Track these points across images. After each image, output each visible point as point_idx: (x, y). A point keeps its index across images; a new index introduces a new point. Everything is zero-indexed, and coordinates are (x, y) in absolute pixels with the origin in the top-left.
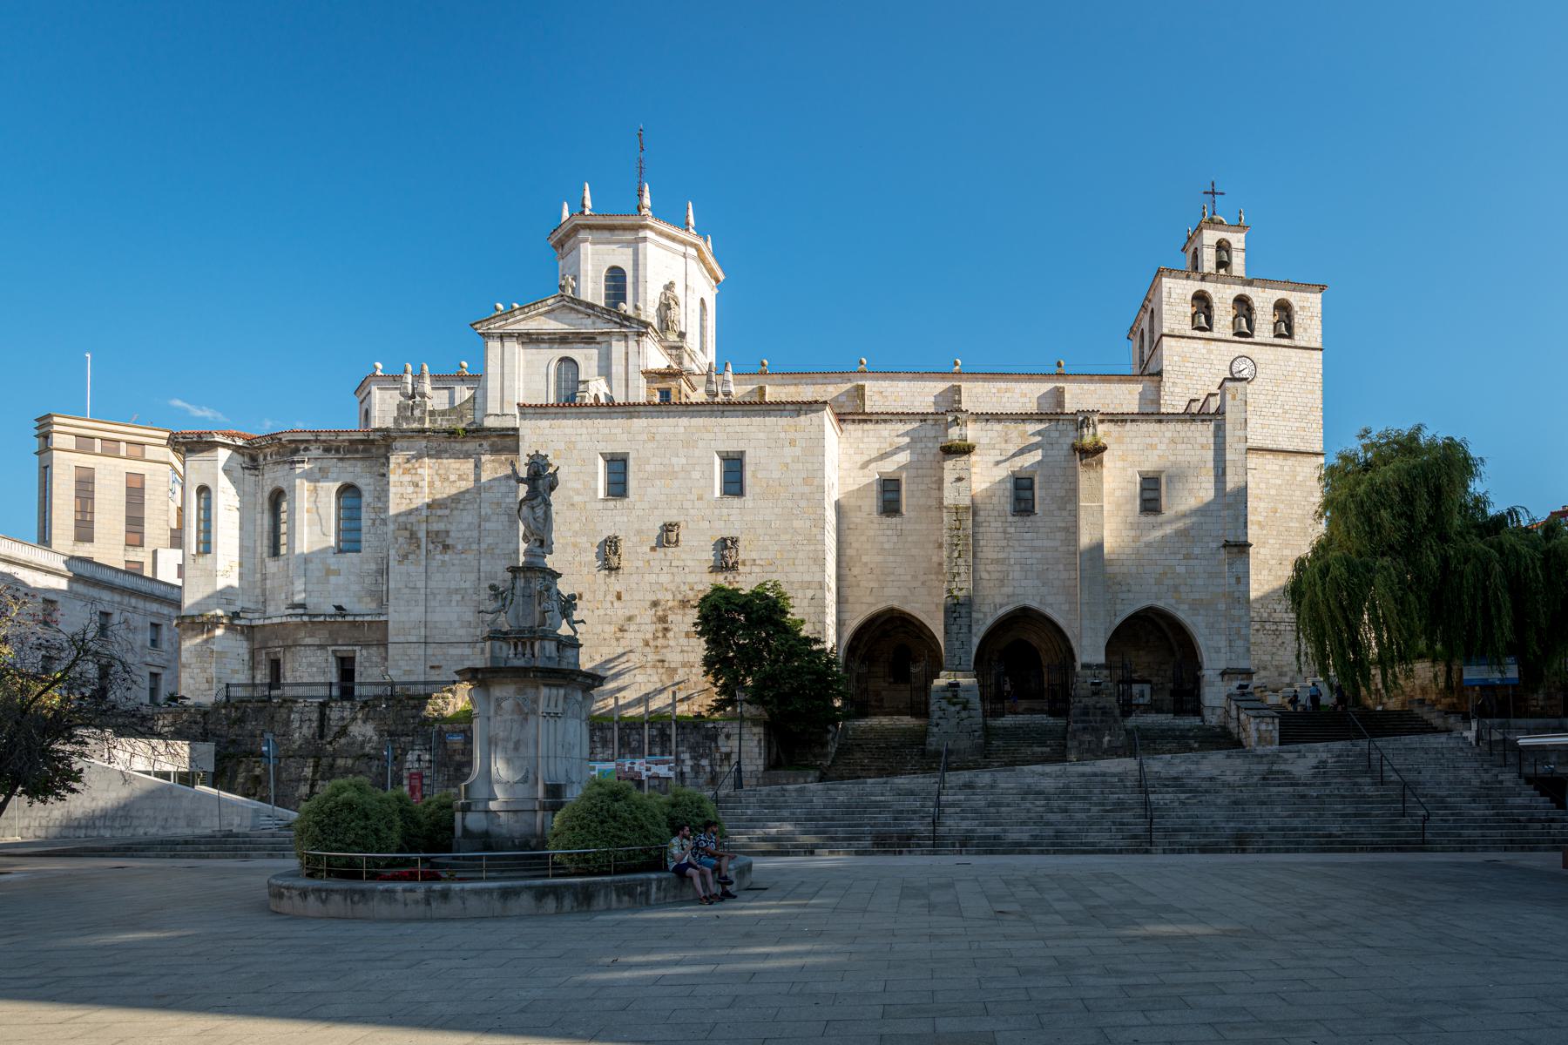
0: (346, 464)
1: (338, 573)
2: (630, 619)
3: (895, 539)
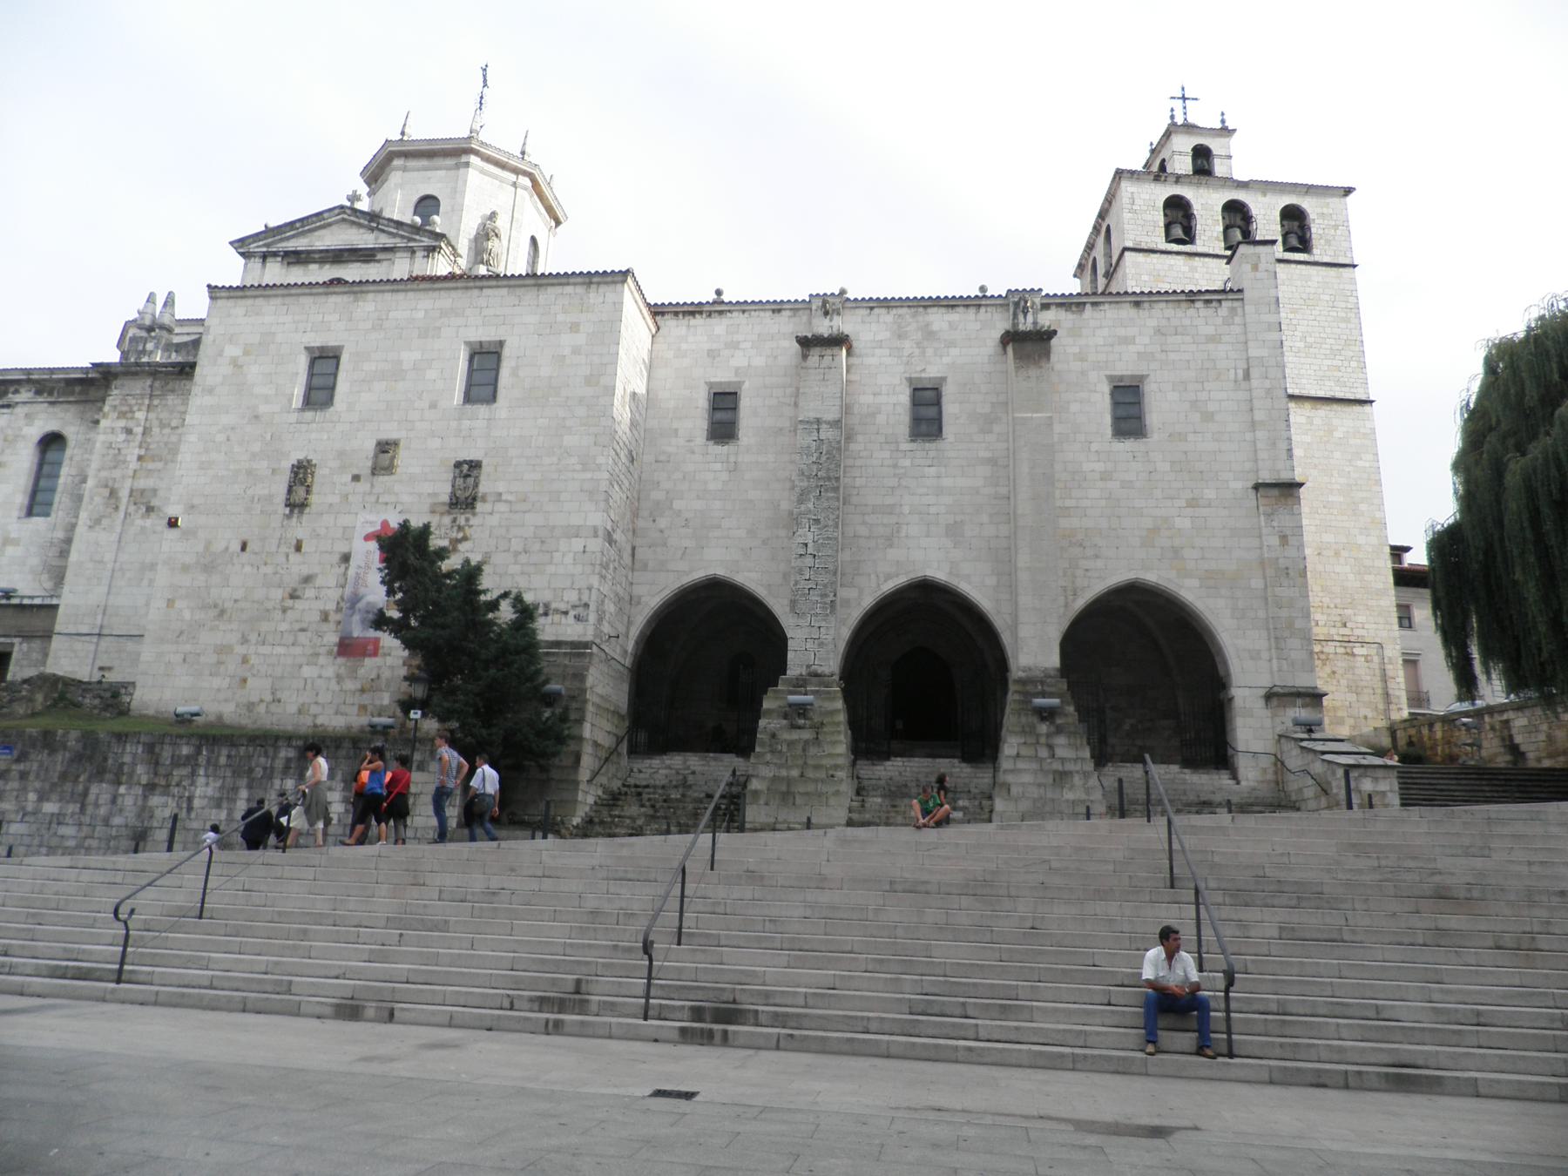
0: (57, 409)
1: (15, 542)
2: (307, 579)
3: (725, 476)
